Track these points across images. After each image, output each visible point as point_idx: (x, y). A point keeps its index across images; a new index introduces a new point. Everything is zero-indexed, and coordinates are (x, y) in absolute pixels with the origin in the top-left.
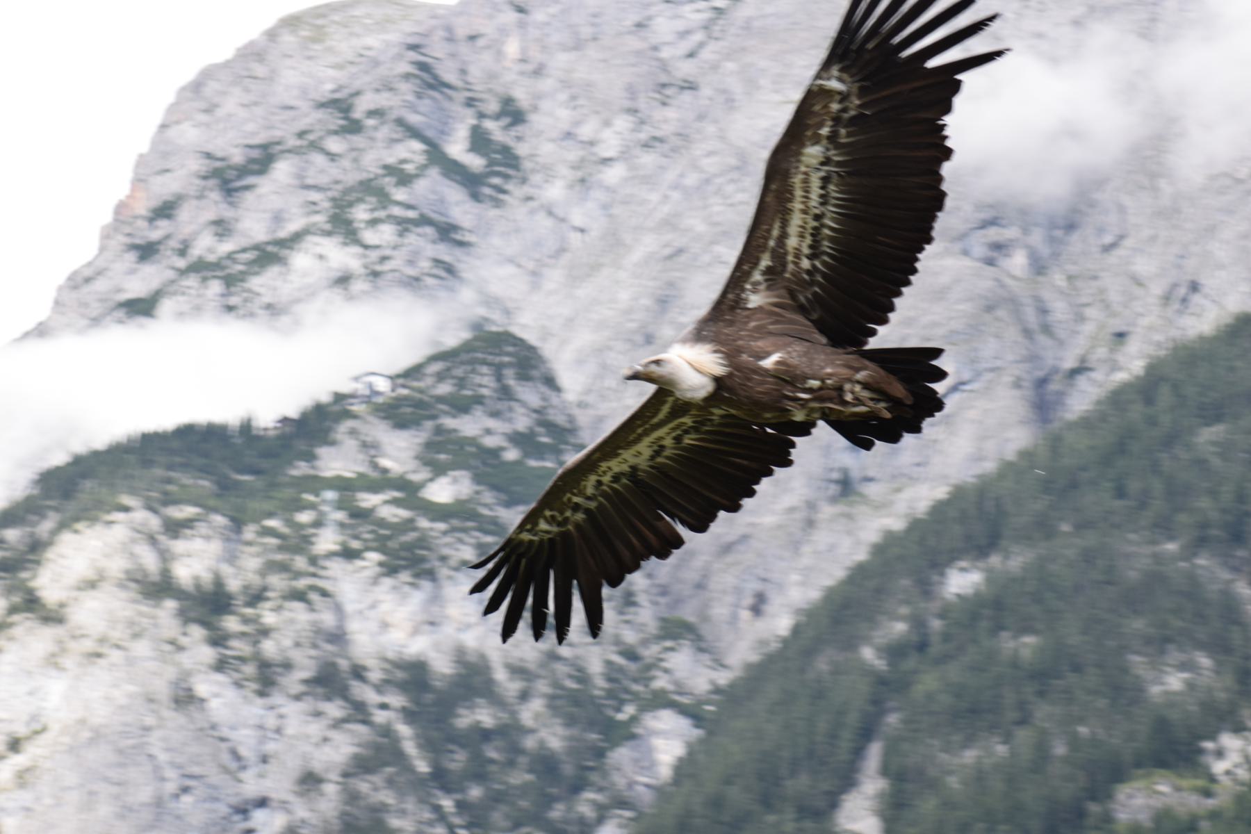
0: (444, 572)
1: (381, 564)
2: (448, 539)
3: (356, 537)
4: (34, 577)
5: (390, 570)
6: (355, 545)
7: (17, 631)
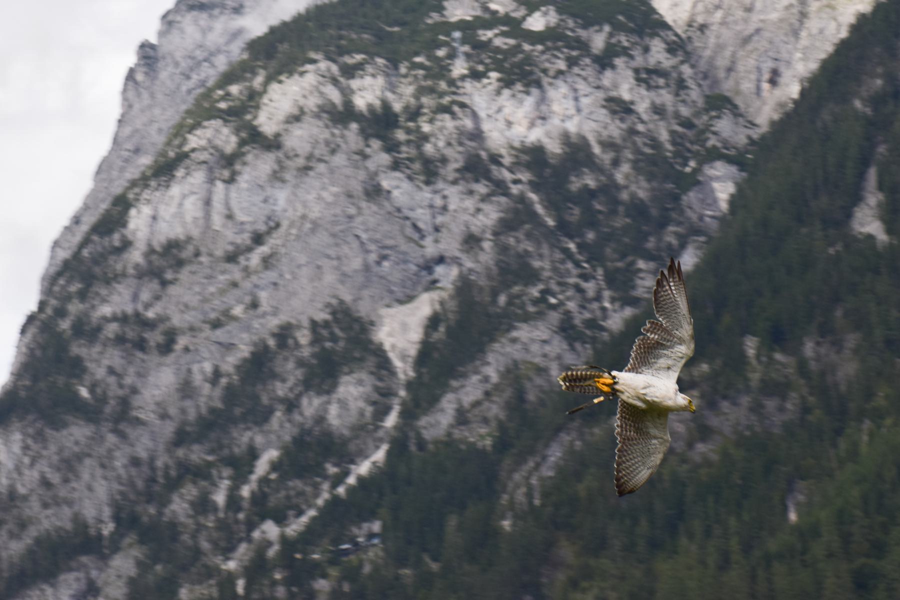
0: (545, 80)
1: (499, 80)
2: (545, 57)
3: (481, 62)
4: (255, 117)
5: (507, 83)
6: (481, 68)
7: (249, 158)
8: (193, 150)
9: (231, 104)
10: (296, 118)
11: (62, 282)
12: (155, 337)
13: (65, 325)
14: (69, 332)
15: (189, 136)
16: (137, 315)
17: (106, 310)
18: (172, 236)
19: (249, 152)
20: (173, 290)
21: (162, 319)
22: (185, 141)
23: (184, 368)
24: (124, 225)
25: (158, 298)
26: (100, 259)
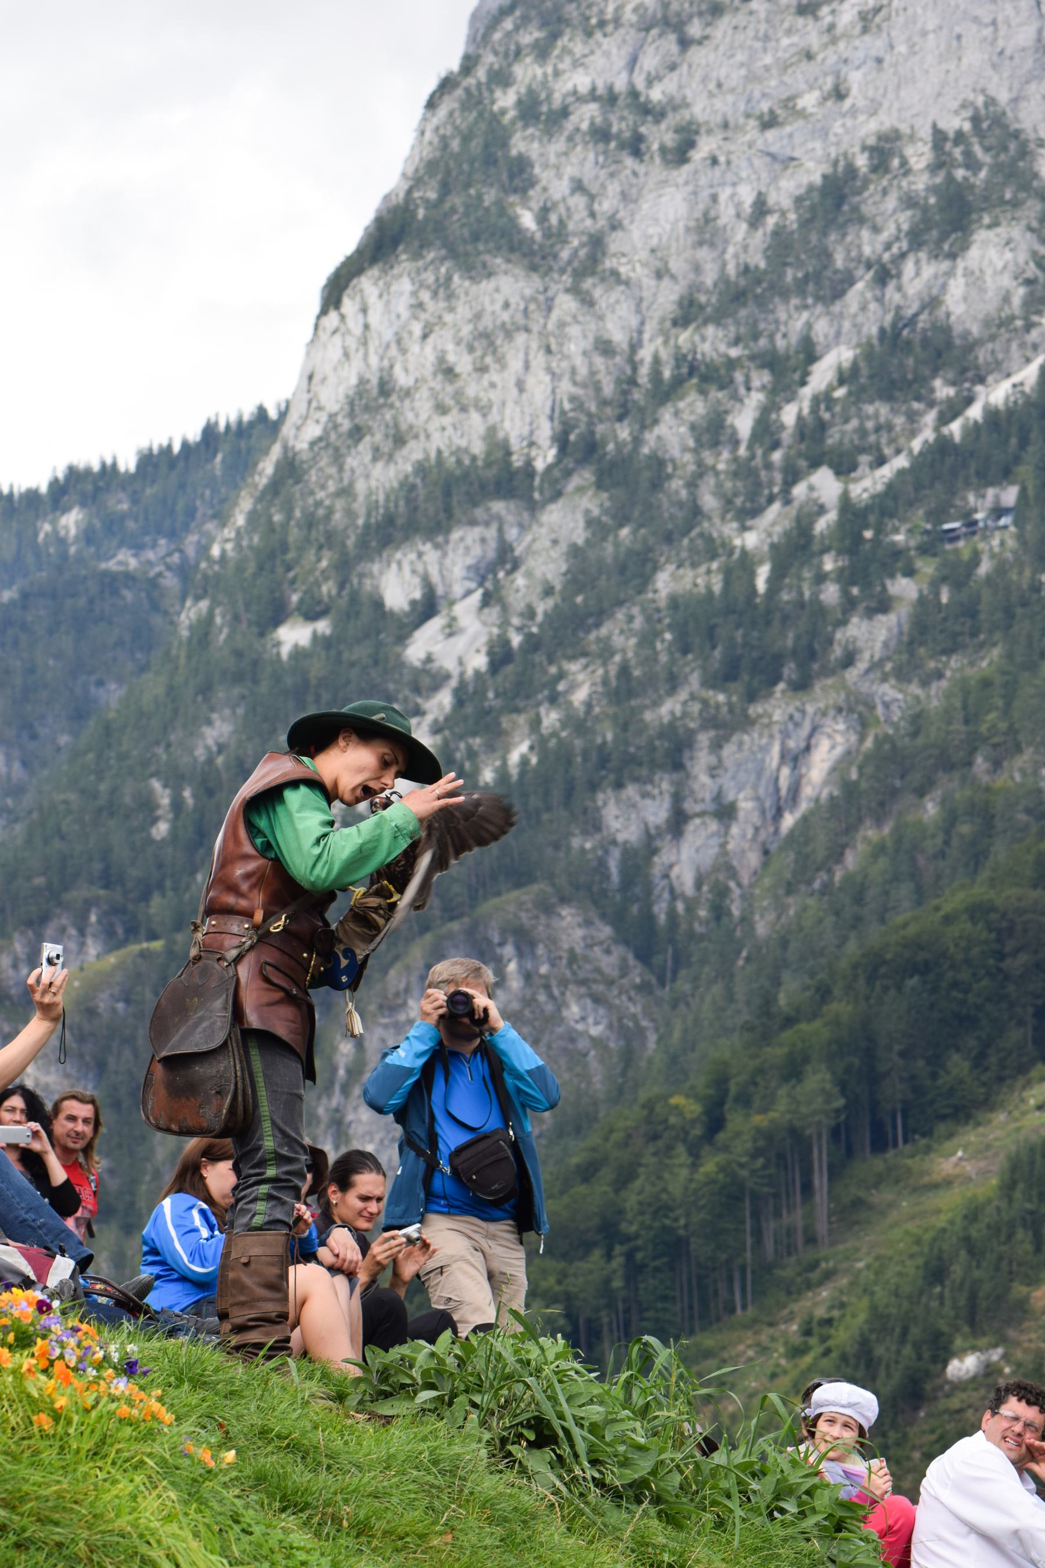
11: (508, 24)
13: (506, 100)
14: (512, 114)
16: (634, 94)
17: (581, 81)
20: (696, 54)
21: (675, 105)
23: (705, 194)
25: (673, 67)
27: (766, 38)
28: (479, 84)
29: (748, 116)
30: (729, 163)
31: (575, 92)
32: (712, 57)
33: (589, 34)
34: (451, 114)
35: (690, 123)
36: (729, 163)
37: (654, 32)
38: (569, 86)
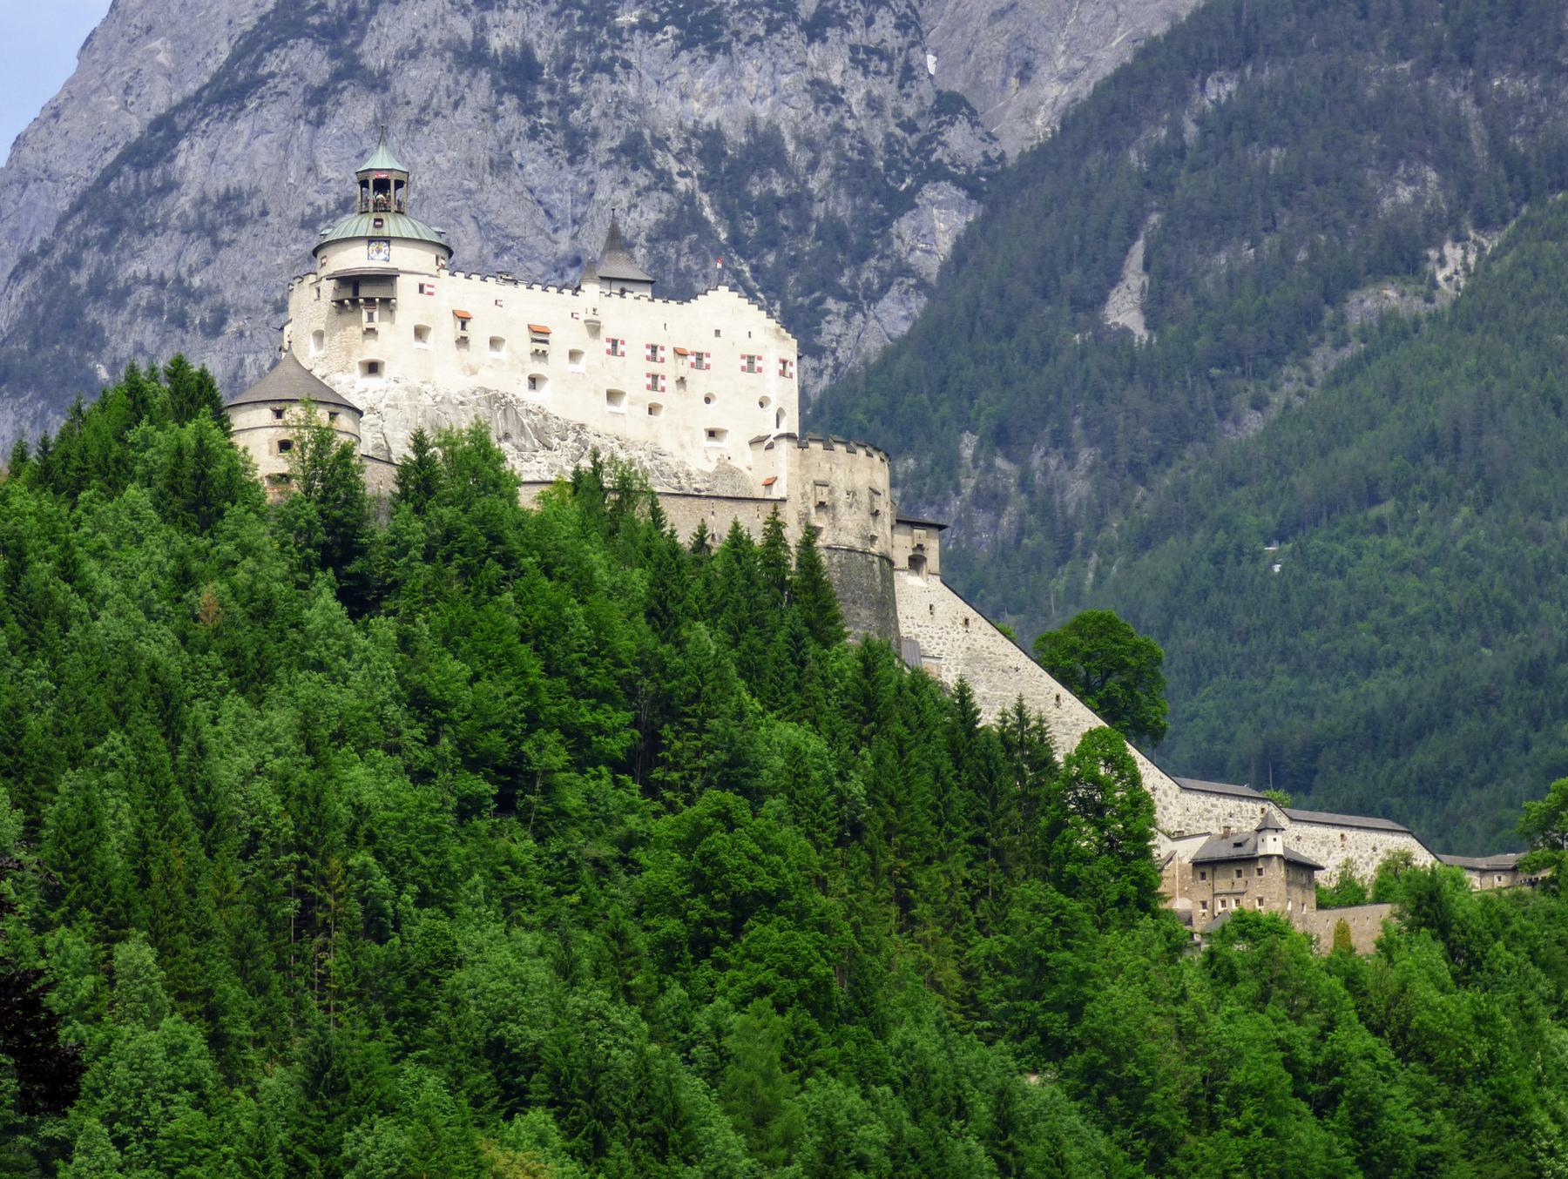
0: (736, 47)
1: (675, 37)
2: (737, 15)
3: (655, 10)
4: (355, 44)
5: (686, 43)
6: (655, 18)
7: (347, 95)
8: (272, 75)
9: (326, 18)
10: (412, 54)
11: (78, 219)
12: (199, 314)
13: (81, 279)
14: (84, 289)
15: (267, 55)
16: (179, 280)
17: (138, 268)
18: (234, 183)
19: (344, 88)
20: (225, 253)
21: (208, 291)
22: (260, 59)
23: (235, 357)
24: (172, 159)
25: (208, 262)
26: (135, 199)
27: (279, 244)
28: (56, 265)
29: (265, 302)
30: (252, 336)
31: (135, 276)
32: (238, 256)
33: (143, 233)
34: (34, 285)
35: (223, 305)
36: (252, 336)
37: (194, 235)
38: (130, 271)
